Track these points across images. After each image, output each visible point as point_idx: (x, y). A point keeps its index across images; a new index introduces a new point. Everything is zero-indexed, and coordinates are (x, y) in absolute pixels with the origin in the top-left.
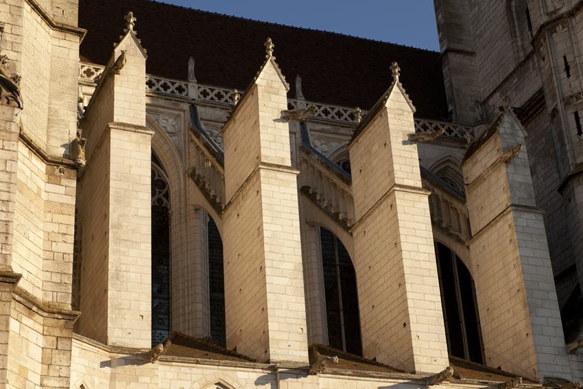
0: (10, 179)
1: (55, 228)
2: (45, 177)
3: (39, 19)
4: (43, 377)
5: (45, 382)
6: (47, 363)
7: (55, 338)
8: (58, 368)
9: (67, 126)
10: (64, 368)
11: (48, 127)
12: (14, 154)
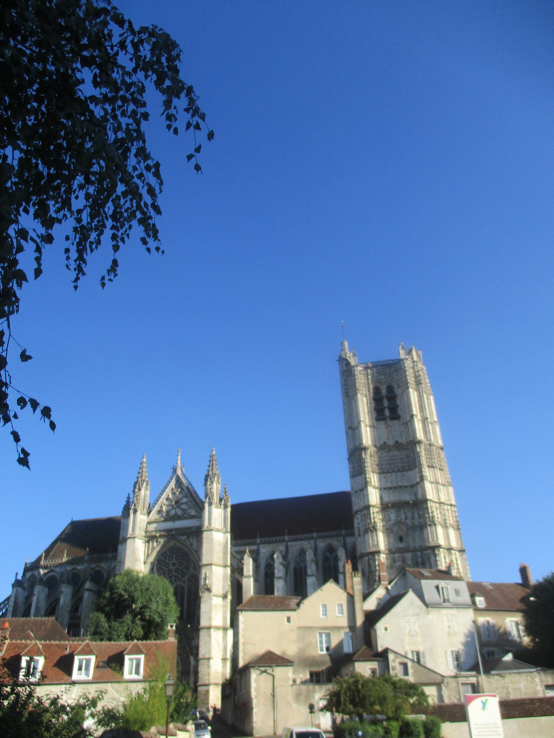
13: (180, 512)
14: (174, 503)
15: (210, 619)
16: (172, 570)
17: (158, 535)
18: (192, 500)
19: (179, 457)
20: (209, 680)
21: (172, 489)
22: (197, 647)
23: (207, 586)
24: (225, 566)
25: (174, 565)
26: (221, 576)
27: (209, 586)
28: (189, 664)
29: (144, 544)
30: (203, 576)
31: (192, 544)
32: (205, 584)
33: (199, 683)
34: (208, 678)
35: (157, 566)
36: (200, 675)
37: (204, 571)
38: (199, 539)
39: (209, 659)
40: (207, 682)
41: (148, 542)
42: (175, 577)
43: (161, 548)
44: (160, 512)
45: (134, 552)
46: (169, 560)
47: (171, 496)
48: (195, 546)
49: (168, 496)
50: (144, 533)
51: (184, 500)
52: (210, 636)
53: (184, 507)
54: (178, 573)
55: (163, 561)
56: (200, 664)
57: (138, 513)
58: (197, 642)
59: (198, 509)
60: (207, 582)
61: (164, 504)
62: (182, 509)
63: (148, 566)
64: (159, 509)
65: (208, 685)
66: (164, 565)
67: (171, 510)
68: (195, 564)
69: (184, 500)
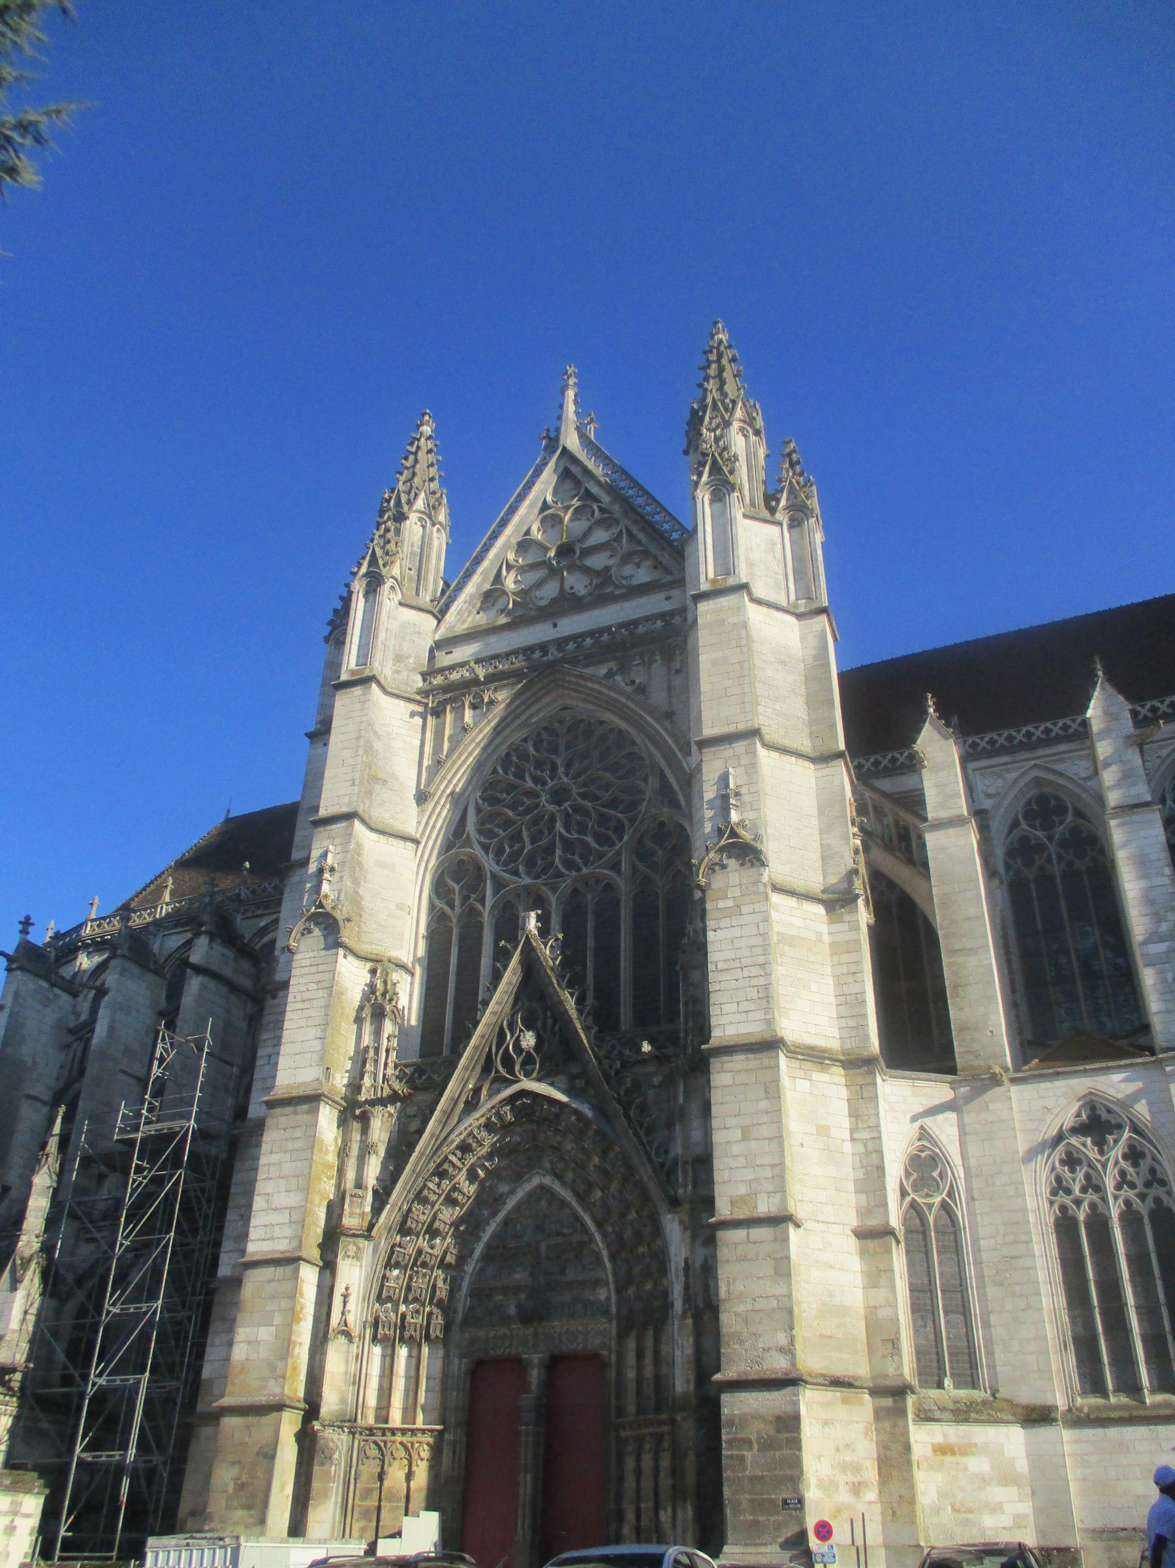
0: (764, 940)
1: (844, 969)
2: (825, 919)
3: (793, 759)
4: (852, 1131)
5: (855, 1136)
6: (854, 1114)
7: (858, 1087)
8: (865, 1118)
9: (842, 858)
10: (872, 1118)
11: (823, 865)
12: (765, 914)
13: (577, 583)
14: (552, 554)
15: (766, 997)
16: (553, 819)
17: (481, 673)
18: (635, 531)
19: (570, 394)
20: (788, 1350)
21: (545, 506)
22: (703, 1163)
23: (733, 834)
24: (823, 758)
25: (559, 796)
26: (810, 805)
27: (747, 836)
28: (660, 1258)
29: (418, 721)
30: (709, 792)
31: (642, 690)
32: (726, 830)
33: (729, 1372)
34: (782, 1339)
35: (479, 810)
36: (729, 1320)
37: (712, 767)
38: (677, 664)
39: (781, 1220)
40: (778, 1364)
41: (438, 713)
42: (568, 845)
43: (497, 731)
44: (489, 598)
45: (365, 741)
46: (537, 780)
47: (537, 534)
48: (658, 697)
49: (528, 532)
50: (419, 678)
51: (600, 536)
52: (772, 1090)
53: (597, 561)
54: (583, 830)
55: (511, 788)
56: (723, 1253)
57: (388, 599)
58: (696, 1135)
59: (665, 558)
60: (734, 816)
61: (509, 567)
62: (587, 570)
63: (441, 813)
64: (487, 586)
65: (790, 1381)
66: (513, 806)
67: (540, 584)
68: (662, 775)
69: (600, 536)
